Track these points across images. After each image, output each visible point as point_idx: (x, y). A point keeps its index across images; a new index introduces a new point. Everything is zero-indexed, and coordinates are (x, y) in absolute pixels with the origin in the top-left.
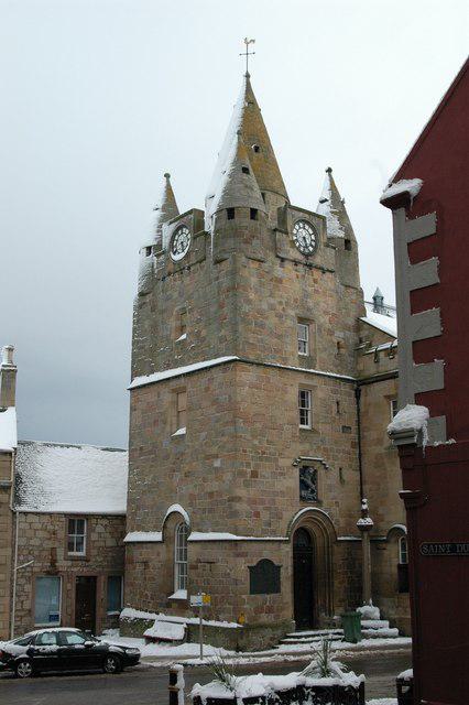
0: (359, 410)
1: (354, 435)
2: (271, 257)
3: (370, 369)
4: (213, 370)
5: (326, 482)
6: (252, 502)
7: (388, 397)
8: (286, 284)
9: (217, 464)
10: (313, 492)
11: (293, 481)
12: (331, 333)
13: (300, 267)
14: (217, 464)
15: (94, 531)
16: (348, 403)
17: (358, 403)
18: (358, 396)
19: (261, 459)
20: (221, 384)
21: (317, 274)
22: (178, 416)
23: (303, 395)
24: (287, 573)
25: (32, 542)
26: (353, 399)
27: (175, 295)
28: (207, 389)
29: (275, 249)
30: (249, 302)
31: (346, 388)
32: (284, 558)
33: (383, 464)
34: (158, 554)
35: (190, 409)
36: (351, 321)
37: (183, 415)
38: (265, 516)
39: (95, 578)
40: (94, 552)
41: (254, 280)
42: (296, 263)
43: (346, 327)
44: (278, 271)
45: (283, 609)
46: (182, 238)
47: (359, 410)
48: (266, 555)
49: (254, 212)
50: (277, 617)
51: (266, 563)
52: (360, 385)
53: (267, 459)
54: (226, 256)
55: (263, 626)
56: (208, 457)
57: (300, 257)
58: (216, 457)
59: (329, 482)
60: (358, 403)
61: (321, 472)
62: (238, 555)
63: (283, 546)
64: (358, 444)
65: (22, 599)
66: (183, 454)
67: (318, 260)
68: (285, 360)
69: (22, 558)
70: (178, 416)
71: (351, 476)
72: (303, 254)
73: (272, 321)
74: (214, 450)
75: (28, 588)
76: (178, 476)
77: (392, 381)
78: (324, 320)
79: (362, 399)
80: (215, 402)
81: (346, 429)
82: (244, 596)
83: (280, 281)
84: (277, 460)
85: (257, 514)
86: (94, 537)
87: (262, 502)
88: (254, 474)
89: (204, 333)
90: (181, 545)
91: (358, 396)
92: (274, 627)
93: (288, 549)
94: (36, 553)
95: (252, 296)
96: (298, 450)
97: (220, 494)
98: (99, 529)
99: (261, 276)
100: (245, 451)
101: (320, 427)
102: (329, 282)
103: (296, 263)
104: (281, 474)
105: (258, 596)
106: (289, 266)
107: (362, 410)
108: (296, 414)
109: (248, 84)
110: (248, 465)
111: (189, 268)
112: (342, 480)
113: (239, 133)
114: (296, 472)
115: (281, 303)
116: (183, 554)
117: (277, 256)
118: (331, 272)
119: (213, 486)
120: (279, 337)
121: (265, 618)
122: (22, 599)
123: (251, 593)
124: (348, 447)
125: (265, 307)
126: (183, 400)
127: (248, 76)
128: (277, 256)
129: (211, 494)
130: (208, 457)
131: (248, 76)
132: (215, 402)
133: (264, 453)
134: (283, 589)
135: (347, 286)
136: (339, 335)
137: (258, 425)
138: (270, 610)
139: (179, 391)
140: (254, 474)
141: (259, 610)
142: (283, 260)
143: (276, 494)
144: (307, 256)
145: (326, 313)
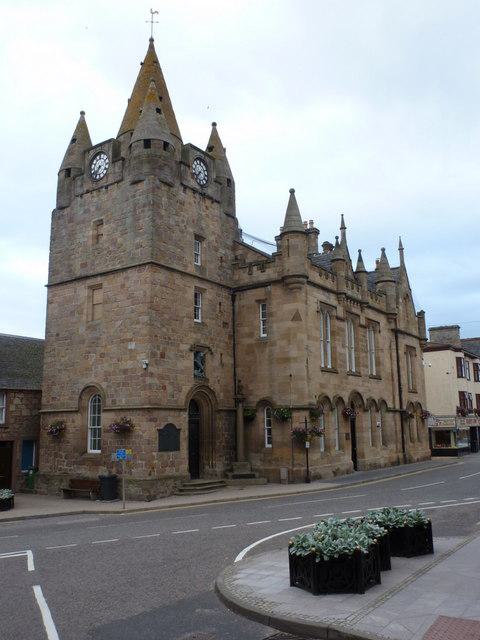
0: (233, 310)
1: (230, 329)
2: (177, 184)
3: (244, 278)
4: (129, 271)
5: (212, 363)
6: (161, 377)
7: (259, 301)
8: (187, 206)
9: (132, 346)
10: (202, 371)
11: (188, 362)
12: (217, 250)
13: (197, 196)
14: (132, 346)
15: (12, 403)
16: (227, 304)
17: (233, 305)
18: (233, 300)
20: (136, 282)
21: (208, 202)
22: (93, 308)
23: (196, 296)
24: (184, 435)
26: (230, 303)
27: (93, 209)
28: (123, 286)
29: (180, 176)
30: (161, 217)
31: (225, 293)
32: (182, 421)
33: (253, 352)
34: (73, 422)
35: (105, 302)
36: (230, 243)
37: (99, 309)
38: (170, 389)
39: (12, 442)
40: (12, 421)
41: (164, 200)
42: (194, 191)
43: (226, 247)
44: (181, 195)
46: (100, 162)
47: (233, 310)
48: (171, 420)
49: (166, 145)
50: (177, 470)
51: (171, 426)
52: (235, 292)
54: (142, 178)
55: (170, 478)
56: (123, 341)
57: (198, 187)
58: (131, 340)
60: (233, 305)
61: (208, 356)
62: (151, 420)
64: (233, 336)
66: (98, 339)
67: (209, 191)
68: (186, 266)
70: (93, 308)
71: (228, 360)
72: (199, 184)
73: (176, 235)
74: (129, 335)
76: (93, 357)
77: (263, 289)
78: (212, 238)
79: (237, 303)
80: (130, 297)
81: (225, 324)
82: (154, 454)
83: (182, 203)
85: (164, 388)
86: (12, 408)
88: (163, 356)
89: (119, 240)
90: (94, 413)
91: (233, 300)
92: (175, 478)
93: (185, 415)
95: (163, 212)
96: (193, 338)
97: (133, 370)
98: (17, 401)
99: (169, 198)
101: (207, 321)
102: (216, 210)
103: (194, 191)
105: (165, 454)
106: (190, 193)
107: (237, 310)
108: (192, 309)
109: (151, 47)
111: (106, 187)
113: (129, 100)
114: (192, 355)
115: (183, 222)
116: (97, 421)
117: (182, 184)
118: (218, 202)
119: (128, 364)
120: (182, 249)
121: (169, 471)
123: (160, 450)
124: (226, 340)
125: (172, 222)
126: (99, 296)
127: (152, 40)
128: (182, 184)
129: (125, 371)
130: (123, 341)
131: (152, 40)
132: (130, 297)
135: (228, 215)
136: (222, 251)
138: (173, 464)
139: (93, 288)
140: (163, 356)
141: (165, 465)
142: (185, 187)
144: (202, 186)
145: (214, 233)
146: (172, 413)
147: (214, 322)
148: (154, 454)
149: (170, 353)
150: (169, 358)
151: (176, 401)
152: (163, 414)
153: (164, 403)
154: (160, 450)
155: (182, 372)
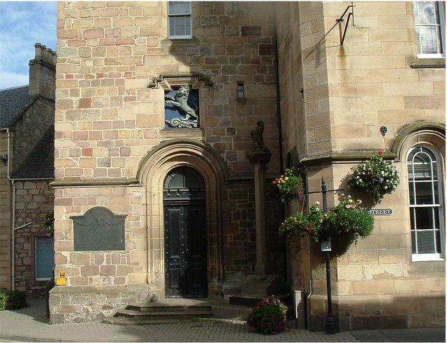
6: (77, 137)
19: (95, 83)
25: (29, 207)
38: (100, 153)
45: (129, 270)
53: (104, 83)
59: (216, 103)
63: (130, 189)
65: (22, 255)
69: (20, 220)
75: (27, 246)
82: (64, 253)
84: (122, 82)
85: (88, 152)
87: (96, 136)
94: (34, 215)
100: (69, 76)
104: (133, 99)
110: (75, 93)
112: (241, 101)
114: (159, 93)
121: (98, 281)
122: (22, 255)
123: (77, 248)
133: (100, 76)
134: (128, 245)
137: (92, 43)
138: (108, 271)
140: (85, 103)
143: (119, 124)
146: (105, 190)
147: (215, 31)
148: (64, 253)
149: (104, 96)
150: (98, 105)
151: (117, 172)
152: (83, 191)
153: (90, 175)
154: (77, 248)
155: (130, 123)
